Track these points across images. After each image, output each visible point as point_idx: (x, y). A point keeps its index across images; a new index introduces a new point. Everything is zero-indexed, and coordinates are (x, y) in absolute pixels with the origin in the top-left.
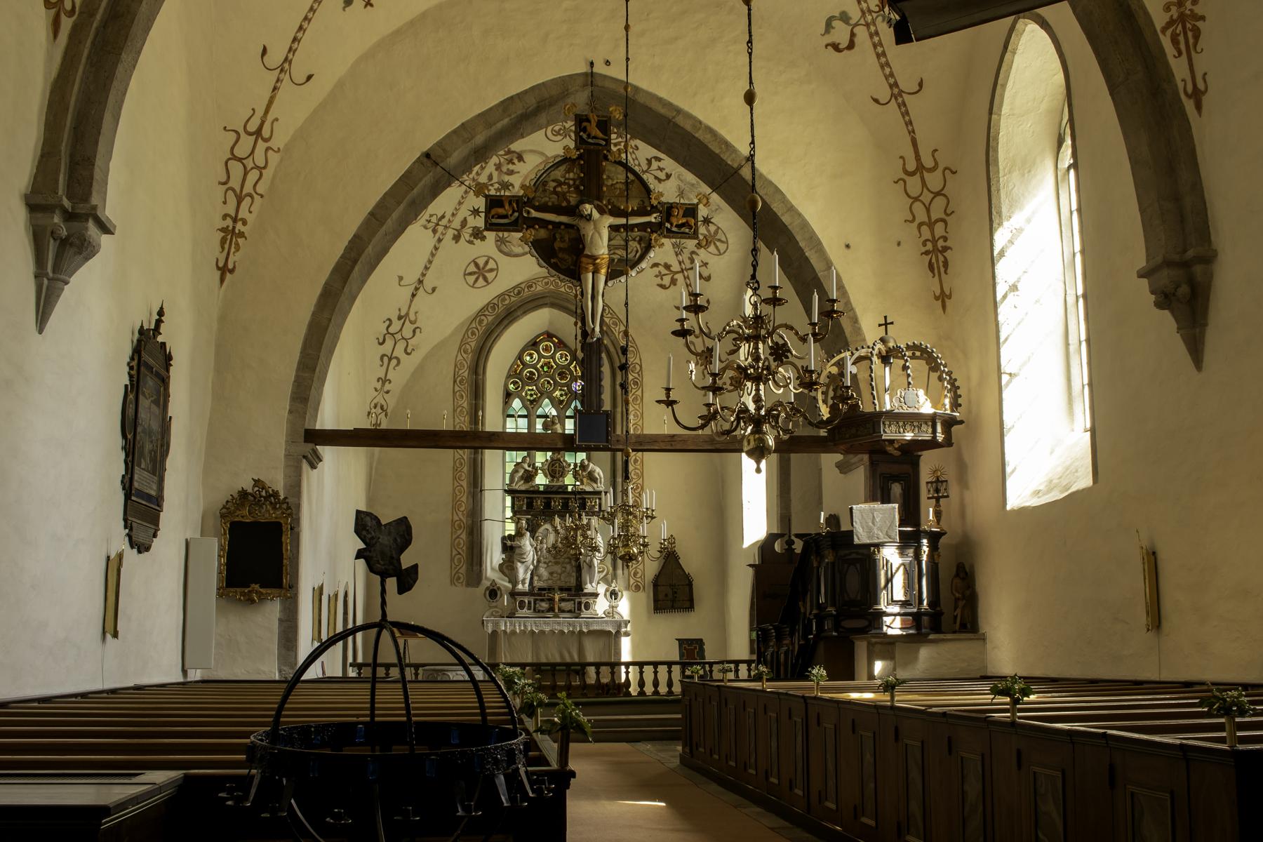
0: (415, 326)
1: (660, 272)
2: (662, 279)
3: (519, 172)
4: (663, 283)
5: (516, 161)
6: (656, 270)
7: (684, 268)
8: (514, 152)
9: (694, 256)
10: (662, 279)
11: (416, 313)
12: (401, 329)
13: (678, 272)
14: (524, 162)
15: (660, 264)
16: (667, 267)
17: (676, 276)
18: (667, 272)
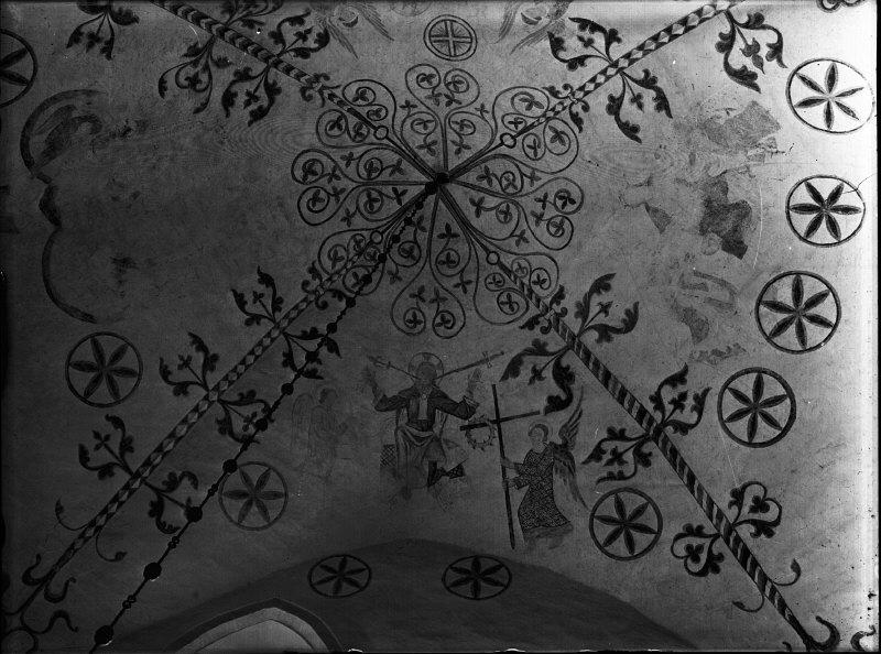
1: (107, 438)
2: (97, 448)
3: (228, 115)
4: (92, 454)
5: (254, 107)
6: (109, 428)
7: (144, 475)
8: (272, 101)
9: (186, 482)
10: (97, 448)
13: (127, 469)
14: (250, 123)
15: (124, 430)
16: (127, 445)
17: (118, 471)
18: (117, 451)
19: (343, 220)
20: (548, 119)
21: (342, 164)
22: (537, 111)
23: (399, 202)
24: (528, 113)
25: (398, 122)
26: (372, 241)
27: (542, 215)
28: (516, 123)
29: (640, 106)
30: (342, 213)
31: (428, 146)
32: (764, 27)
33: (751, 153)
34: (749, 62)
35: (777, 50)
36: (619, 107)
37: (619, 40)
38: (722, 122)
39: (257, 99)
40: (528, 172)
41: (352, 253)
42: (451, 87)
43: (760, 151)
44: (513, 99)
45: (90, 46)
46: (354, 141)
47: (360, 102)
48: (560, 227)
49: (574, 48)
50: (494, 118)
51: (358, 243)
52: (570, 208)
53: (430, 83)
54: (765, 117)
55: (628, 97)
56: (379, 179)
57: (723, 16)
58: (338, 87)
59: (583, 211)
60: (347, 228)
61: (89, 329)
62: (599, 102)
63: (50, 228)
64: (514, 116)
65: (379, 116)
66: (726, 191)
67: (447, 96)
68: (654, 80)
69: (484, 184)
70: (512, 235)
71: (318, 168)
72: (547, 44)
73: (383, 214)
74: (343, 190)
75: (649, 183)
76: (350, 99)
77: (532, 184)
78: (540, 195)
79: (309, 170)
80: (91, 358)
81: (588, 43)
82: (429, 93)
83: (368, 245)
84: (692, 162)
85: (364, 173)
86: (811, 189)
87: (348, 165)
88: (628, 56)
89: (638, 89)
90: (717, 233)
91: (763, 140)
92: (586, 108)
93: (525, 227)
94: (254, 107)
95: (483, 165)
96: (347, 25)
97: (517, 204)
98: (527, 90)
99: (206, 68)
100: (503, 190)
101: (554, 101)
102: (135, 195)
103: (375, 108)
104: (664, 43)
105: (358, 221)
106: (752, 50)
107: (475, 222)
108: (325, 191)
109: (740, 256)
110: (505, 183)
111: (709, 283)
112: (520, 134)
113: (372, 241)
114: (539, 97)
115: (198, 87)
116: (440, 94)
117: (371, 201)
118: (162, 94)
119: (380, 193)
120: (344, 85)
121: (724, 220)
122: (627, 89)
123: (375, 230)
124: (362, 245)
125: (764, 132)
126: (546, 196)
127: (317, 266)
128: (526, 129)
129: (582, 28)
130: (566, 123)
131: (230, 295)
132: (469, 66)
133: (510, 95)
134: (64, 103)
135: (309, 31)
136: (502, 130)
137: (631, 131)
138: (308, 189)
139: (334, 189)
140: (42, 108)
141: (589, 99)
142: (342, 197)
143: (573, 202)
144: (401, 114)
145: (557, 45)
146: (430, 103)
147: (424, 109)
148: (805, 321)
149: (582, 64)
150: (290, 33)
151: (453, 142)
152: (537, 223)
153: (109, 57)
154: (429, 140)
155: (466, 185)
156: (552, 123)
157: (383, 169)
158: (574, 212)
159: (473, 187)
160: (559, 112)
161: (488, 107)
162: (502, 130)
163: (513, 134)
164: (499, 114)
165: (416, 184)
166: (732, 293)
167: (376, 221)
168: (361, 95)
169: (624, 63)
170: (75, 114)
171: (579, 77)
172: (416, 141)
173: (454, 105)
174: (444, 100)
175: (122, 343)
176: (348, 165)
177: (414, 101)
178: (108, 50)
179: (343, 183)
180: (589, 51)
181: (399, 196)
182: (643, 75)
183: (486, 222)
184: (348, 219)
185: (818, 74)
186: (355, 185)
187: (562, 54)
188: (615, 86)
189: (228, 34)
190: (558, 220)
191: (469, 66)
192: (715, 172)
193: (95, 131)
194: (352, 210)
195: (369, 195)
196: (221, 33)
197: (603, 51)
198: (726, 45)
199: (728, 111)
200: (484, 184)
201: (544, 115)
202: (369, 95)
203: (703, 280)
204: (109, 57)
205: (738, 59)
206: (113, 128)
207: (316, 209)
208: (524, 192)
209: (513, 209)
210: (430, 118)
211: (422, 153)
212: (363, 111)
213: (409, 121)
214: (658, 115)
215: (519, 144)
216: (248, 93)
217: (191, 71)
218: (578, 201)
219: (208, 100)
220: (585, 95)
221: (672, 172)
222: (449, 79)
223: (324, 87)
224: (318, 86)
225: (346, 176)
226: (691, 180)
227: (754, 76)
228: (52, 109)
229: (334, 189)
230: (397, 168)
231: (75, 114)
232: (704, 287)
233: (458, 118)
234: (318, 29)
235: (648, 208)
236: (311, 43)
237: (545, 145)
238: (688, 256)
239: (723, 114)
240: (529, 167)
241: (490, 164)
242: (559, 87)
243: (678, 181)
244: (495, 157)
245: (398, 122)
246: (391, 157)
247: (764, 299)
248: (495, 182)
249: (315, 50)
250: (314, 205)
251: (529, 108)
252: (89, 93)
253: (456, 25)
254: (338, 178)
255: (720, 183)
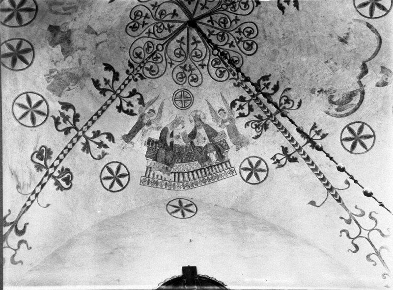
0: (367, 214)
3: (278, 82)
5: (267, 82)
11: (356, 207)
12: (360, 227)
19: (239, 20)
20: (143, 62)
21: (235, 44)
22: (148, 66)
23: (211, 18)
24: (151, 64)
25: (208, 57)
26: (227, 6)
27: (145, 19)
28: (157, 58)
29: (105, 80)
30: (239, 23)
31: (196, 42)
32: (63, 130)
33: (55, 73)
34: (66, 113)
35: (57, 123)
36: (114, 77)
37: (117, 107)
38: (71, 84)
39: (264, 84)
40: (152, 36)
41: (238, 4)
42: (184, 75)
43: (53, 75)
44: (158, 71)
45: (320, 131)
46: (228, 52)
47: (223, 70)
48: (136, 15)
49: (134, 100)
50: (166, 60)
51: (234, 7)
52: (132, 25)
53: (193, 77)
54: (53, 91)
55: (111, 83)
56: (219, 31)
57: (80, 129)
58: (231, 79)
59: (126, 24)
60: (238, 16)
61: (370, 21)
62: (123, 76)
63: (368, 64)
64: (157, 62)
65: (216, 61)
66: (63, 50)
67: (186, 70)
68: (101, 93)
69: (171, 24)
70: (159, 6)
71: (246, 46)
72: (146, 101)
73: (220, 16)
74: (237, 32)
75: (97, 45)
76: (227, 72)
77: (149, 30)
78: (146, 26)
79: (250, 46)
80: (377, 9)
81: (129, 104)
82: (194, 72)
83: (230, 5)
84: (80, 60)
85: (226, 35)
86: (25, 62)
87: (232, 42)
88: (113, 101)
89: (108, 87)
90: (63, 32)
91: (53, 80)
92: (127, 72)
93: (153, 11)
94: (267, 82)
95: (171, 32)
96: (224, 110)
97: (156, 19)
98: (152, 77)
99: (281, 104)
100: (162, 24)
101: (141, 72)
102: (327, 62)
103: (217, 66)
104: (99, 110)
105: (232, 17)
106: (66, 119)
107: (176, 7)
108: (244, 35)
109: (50, 26)
110: (162, 27)
111: (63, 11)
112: (155, 52)
113: (227, 6)
114: (147, 73)
115: (286, 98)
116: (189, 71)
117: (225, 23)
118: (301, 101)
119: (220, 25)
120: (228, 80)
121: (61, 37)
122: (111, 85)
123: (225, 10)
124: (232, 6)
125: (53, 84)
126: (143, 26)
127: (255, 4)
128: (152, 55)
129: (132, 111)
130: (135, 62)
131: (300, 8)
132: (177, 87)
133: (160, 73)
134: (339, 113)
135: (238, 109)
136: (163, 53)
137: (108, 67)
138: (252, 38)
139: (240, 35)
140: (348, 114)
141: (126, 76)
142: (237, 30)
143: (130, 27)
144: (206, 62)
145: (141, 101)
146: (193, 67)
147: (196, 63)
148: (12, 8)
149: (130, 92)
150: (246, 111)
151: (185, 44)
152: (147, 14)
153: (315, 124)
154: (195, 45)
155: (180, 22)
156: (142, 60)
157: (217, 34)
158: (130, 23)
159: (176, 21)
160: (139, 66)
161: (169, 65)
162: (163, 53)
163: (158, 52)
164: (164, 62)
165: (203, 24)
166: (51, 10)
167: (223, 14)
168: (222, 73)
169: (114, 96)
170: (336, 107)
171: (132, 85)
172: (201, 46)
173: (183, 65)
174: (188, 68)
175: (359, 10)
176: (232, 42)
177: (200, 67)
178: (314, 126)
179: (237, 35)
180: (128, 100)
181: (211, 20)
182: (106, 93)
183: (174, 45)
184: (237, 20)
185: (39, 119)
186: (231, 32)
187: (139, 96)
188: (117, 85)
189: (269, 114)
190: (137, 18)
191: (177, 87)
192: (70, 58)
193: (332, 97)
194: (234, 23)
195: (225, 26)
196: (271, 116)
197: (123, 101)
198: (76, 117)
199: (70, 90)
200: (171, 24)
201: (145, 64)
202: (218, 73)
203: (66, 12)
204: (315, 124)
205: (70, 113)
206: (324, 95)
207: (250, 29)
208: (153, 25)
209: (158, 16)
210: (193, 58)
211: (199, 39)
212: (222, 65)
213: (203, 58)
214: (98, 78)
215: (155, 47)
216: (268, 88)
217: (287, 106)
218: (128, 28)
219: (284, 92)
220: (128, 77)
221: (88, 53)
222: (184, 80)
223: (236, 80)
224: (239, 81)
225: (234, 37)
226: (79, 51)
227: (63, 108)
228: (343, 113)
229: (240, 35)
230: (211, 33)
231: (336, 107)
232: (65, 9)
233: (182, 58)
234: (235, 109)
235: (96, 33)
236: (238, 103)
237: (144, 50)
238: (75, 20)
239: (71, 88)
240: (152, 38)
241: (168, 33)
242: (139, 79)
243: (84, 49)
244: (166, 38)
245: (208, 57)
246: (214, 39)
247: (35, 12)
248: (166, 26)
249: (237, 100)
250: (251, 31)
251: (152, 67)
252: (327, 113)
253: (181, 106)
254: (238, 38)
255: (66, 53)
